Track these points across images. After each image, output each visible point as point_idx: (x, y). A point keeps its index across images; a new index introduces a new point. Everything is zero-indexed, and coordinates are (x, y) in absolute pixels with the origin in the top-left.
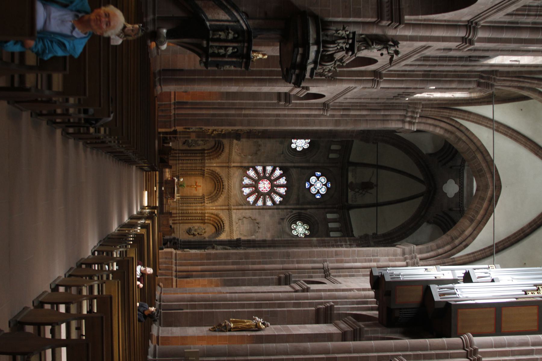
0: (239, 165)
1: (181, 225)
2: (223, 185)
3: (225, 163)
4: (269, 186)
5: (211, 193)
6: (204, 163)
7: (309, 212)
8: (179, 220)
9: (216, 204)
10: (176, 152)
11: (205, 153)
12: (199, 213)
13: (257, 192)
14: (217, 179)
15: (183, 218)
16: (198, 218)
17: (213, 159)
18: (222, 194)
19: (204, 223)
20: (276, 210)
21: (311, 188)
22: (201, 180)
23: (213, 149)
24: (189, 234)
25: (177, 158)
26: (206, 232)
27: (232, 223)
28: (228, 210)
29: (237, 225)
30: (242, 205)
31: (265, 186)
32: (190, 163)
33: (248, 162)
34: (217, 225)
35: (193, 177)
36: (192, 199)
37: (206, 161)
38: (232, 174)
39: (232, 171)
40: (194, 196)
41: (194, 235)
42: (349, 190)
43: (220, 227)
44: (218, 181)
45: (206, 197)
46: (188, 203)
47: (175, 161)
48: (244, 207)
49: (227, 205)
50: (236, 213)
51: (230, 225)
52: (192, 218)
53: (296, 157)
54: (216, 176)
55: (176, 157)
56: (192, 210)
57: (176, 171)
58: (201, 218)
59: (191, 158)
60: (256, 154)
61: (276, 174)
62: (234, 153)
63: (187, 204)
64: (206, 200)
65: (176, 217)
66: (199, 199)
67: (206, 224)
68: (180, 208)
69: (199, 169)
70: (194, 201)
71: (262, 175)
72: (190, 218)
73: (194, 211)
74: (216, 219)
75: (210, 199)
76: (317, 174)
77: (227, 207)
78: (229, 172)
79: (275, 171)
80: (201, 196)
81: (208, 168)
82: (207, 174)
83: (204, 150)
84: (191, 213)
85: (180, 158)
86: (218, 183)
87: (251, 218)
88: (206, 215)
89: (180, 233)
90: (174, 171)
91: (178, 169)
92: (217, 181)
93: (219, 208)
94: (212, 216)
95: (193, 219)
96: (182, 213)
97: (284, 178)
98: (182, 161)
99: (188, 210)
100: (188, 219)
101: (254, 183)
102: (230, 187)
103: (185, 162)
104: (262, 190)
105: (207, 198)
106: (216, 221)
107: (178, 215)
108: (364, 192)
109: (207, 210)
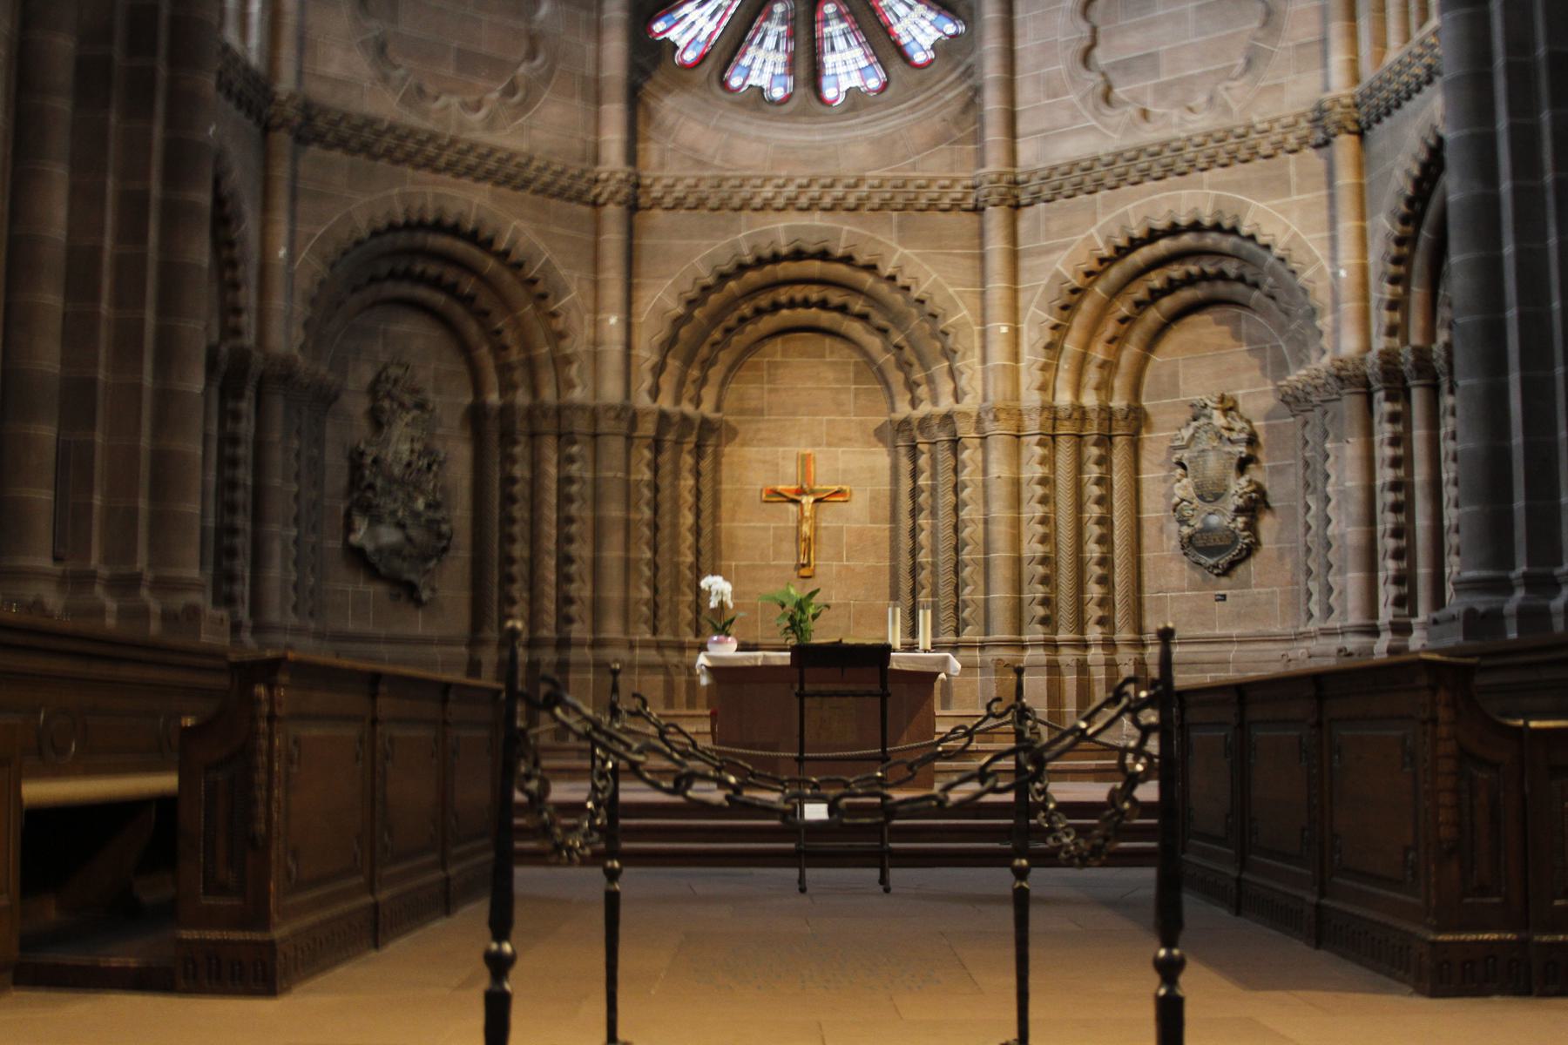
0: (614, 113)
2: (798, 255)
3: (597, 232)
5: (872, 371)
6: (594, 414)
8: (1109, 644)
9: (962, 315)
11: (507, 411)
12: (1042, 462)
15: (1093, 612)
16: (1093, 472)
18: (871, 268)
19: (1137, 419)
22: (751, 452)
23: (472, 329)
24: (1251, 550)
27: (1141, 150)
28: (1017, 207)
29: (1155, 110)
30: (977, 91)
32: (598, 544)
33: (597, 31)
34: (1155, 295)
35: (725, 525)
36: (914, 533)
37: (578, 395)
38: (690, 175)
40: (894, 517)
41: (1255, 505)
43: (1176, 271)
45: (903, 409)
46: (957, 568)
48: (991, 70)
49: (969, 220)
50: (1049, 135)
51: (1168, 170)
52: (1093, 531)
54: (715, 319)
56: (1016, 524)
57: (665, 668)
58: (1093, 452)
59: (550, 530)
62: (507, 139)
64: (925, 409)
65: (1083, 668)
66: (915, 474)
67: (1145, 403)
68: (1001, 632)
69: (655, 468)
70: (933, 513)
72: (1093, 551)
73: (1033, 511)
74: (1104, 309)
75: (918, 375)
77: (995, 218)
78: (678, 204)
81: (648, 381)
82: (697, 402)
83: (476, 416)
84: (1044, 540)
85: (548, 632)
86: (776, 307)
88: (1064, 398)
89: (1235, 631)
90: (670, 689)
91: (652, 656)
92: (759, 312)
93: (997, 286)
95: (1105, 521)
96: (1045, 621)
98: (574, 610)
99: (1018, 561)
100: (1105, 561)
102: (815, 191)
103: (581, 590)
105: (914, 403)
106: (1124, 309)
107: (1067, 657)
109: (1016, 397)
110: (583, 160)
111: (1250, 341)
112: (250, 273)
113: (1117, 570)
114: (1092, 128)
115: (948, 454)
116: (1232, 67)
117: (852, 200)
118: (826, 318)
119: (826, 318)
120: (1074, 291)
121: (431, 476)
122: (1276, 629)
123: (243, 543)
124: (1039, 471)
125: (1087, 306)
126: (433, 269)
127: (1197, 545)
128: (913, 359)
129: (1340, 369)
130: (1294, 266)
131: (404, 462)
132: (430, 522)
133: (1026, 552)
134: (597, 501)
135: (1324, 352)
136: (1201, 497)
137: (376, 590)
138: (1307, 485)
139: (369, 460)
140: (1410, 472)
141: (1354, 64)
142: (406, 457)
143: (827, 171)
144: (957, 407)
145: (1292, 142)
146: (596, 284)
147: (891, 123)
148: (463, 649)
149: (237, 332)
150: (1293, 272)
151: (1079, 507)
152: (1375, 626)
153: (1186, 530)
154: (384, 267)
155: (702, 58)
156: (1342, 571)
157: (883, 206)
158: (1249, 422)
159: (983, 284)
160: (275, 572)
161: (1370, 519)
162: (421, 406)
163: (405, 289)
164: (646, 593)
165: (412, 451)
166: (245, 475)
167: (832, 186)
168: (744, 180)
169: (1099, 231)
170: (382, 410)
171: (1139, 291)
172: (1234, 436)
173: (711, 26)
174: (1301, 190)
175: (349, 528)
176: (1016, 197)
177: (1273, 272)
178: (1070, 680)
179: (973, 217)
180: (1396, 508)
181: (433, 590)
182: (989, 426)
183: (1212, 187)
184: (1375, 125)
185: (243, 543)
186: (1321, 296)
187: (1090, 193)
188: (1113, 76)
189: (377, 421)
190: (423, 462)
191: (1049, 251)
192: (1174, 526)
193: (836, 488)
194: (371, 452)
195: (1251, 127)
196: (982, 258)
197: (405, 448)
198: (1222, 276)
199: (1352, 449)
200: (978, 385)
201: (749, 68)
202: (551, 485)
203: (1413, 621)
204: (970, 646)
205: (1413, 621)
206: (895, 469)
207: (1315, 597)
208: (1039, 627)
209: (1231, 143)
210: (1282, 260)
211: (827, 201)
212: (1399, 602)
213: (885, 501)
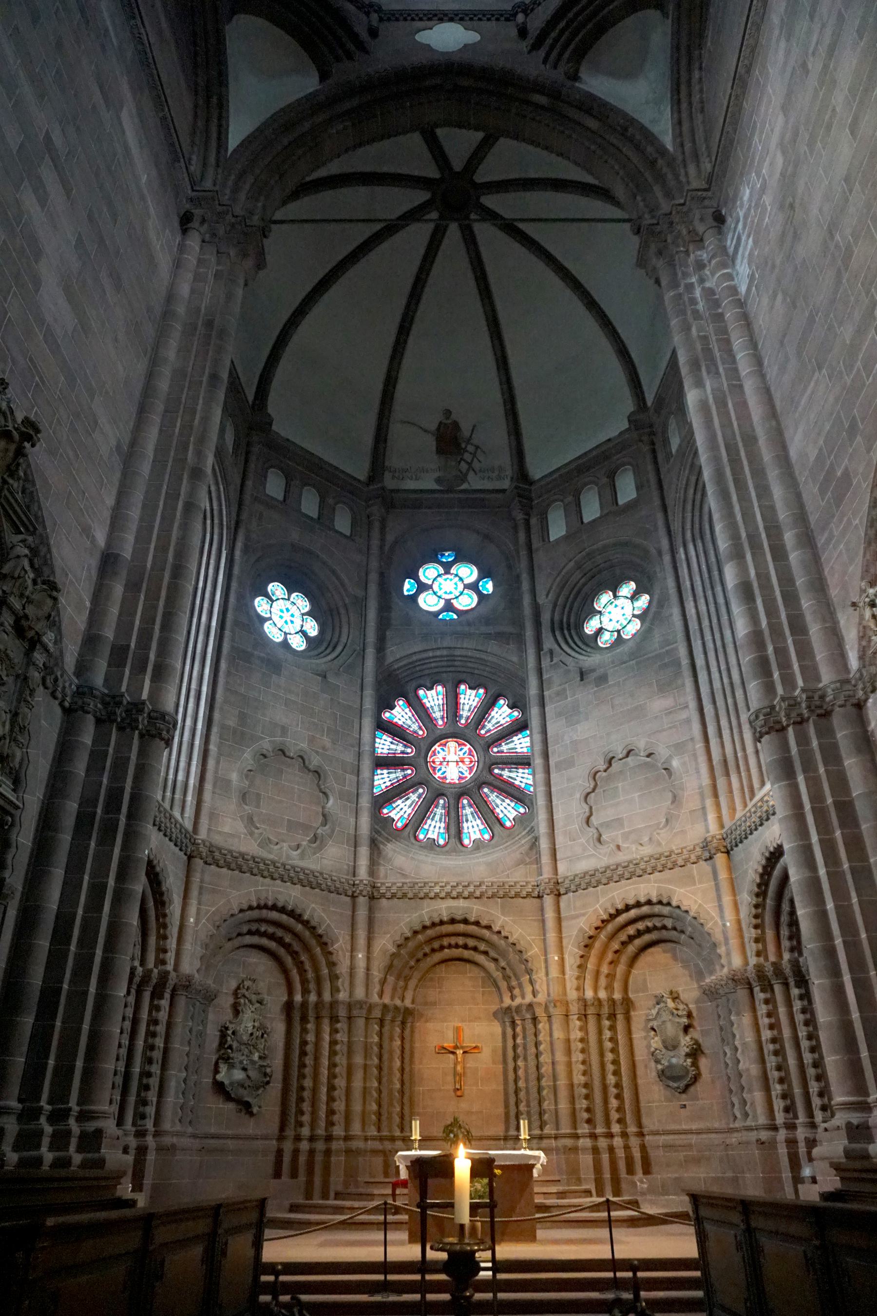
0: (364, 851)
1: (649, 1124)
2: (453, 921)
4: (452, 744)
6: (350, 1006)
7: (547, 595)
8: (624, 1135)
9: (534, 951)
10: (287, 1159)
11: (304, 1005)
12: (581, 1029)
13: (480, 787)
14: (427, 949)
15: (615, 1116)
16: (607, 1034)
17: (332, 965)
18: (488, 927)
19: (628, 1004)
20: (547, 709)
21: (460, 607)
22: (430, 1025)
23: (289, 961)
24: (696, 1078)
25: (320, 1146)
26: (671, 993)
27: (618, 865)
28: (559, 895)
29: (624, 845)
30: (536, 839)
31: (452, 757)
34: (631, 938)
35: (417, 1067)
36: (515, 1070)
38: (400, 881)
39: (388, 879)
40: (505, 1061)
41: (695, 1052)
42: (464, 486)
43: (641, 926)
44: (436, 945)
45: (507, 1001)
46: (540, 1089)
47: (333, 1159)
48: (543, 829)
52: (610, 1068)
53: (344, 639)
54: (412, 955)
55: (312, 1152)
56: (569, 1064)
58: (606, 1023)
59: (324, 1072)
60: (317, 773)
61: (409, 722)
62: (311, 864)
63: (545, 1093)
64: (518, 1001)
65: (611, 1149)
66: (514, 1037)
67: (631, 995)
68: (565, 1130)
69: (380, 1035)
70: (525, 1059)
71: (409, 772)
72: (611, 1079)
73: (578, 1057)
74: (606, 946)
75: (514, 983)
76: (408, 590)
77: (548, 900)
78: (394, 896)
79: (396, 724)
80: (503, 1023)
83: (289, 1007)
84: (584, 1073)
85: (321, 1132)
86: (442, 948)
87: (588, 794)
88: (589, 994)
89: (694, 1126)
91: (377, 1145)
92: (433, 950)
93: (551, 936)
94: (591, 966)
96: (589, 1121)
97: (421, 693)
99: (571, 1086)
100: (618, 1085)
101: (441, 802)
103: (340, 1106)
104: (471, 769)
106: (616, 946)
108: (470, 448)
109: (565, 993)
110: (347, 875)
111: (682, 961)
112: (173, 931)
113: (625, 1090)
114: (593, 855)
115: (531, 1026)
116: (660, 823)
117: (478, 894)
118: (466, 954)
119: (466, 954)
120: (590, 937)
121: (263, 1040)
122: (716, 1125)
123: (154, 1082)
124: (579, 1034)
125: (598, 945)
126: (271, 930)
127: (667, 1075)
128: (512, 975)
129: (734, 975)
130: (702, 921)
131: (250, 1032)
132: (262, 1066)
133: (576, 1081)
134: (350, 1053)
135: (723, 966)
136: (666, 1048)
137: (231, 1106)
138: (723, 1040)
139: (229, 1032)
140: (780, 1031)
141: (720, 818)
142: (250, 1030)
143: (465, 879)
144: (535, 1000)
145: (693, 858)
146: (353, 937)
147: (495, 855)
148: (274, 1142)
149: (163, 962)
150: (702, 924)
151: (602, 1055)
152: (775, 1125)
153: (660, 1067)
154: (245, 929)
155: (406, 825)
156: (750, 1091)
157: (493, 896)
158: (687, 1005)
159: (544, 935)
160: (171, 1098)
161: (762, 1061)
162: (260, 1002)
163: (255, 940)
164: (374, 1107)
165: (254, 1027)
166: (159, 1042)
167: (468, 885)
168: (425, 883)
169: (600, 906)
170: (240, 1004)
171: (623, 937)
172: (680, 1013)
173: (409, 811)
174: (700, 883)
175: (216, 1071)
176: (558, 890)
177: (691, 925)
178: (605, 1157)
179: (538, 900)
180: (776, 1053)
181: (260, 1107)
182: (552, 1010)
183: (655, 882)
184: (735, 849)
185: (154, 1082)
186: (718, 936)
187: (594, 887)
188: (600, 829)
189: (236, 1010)
190: (259, 1033)
191: (577, 917)
192: (653, 1064)
193: (474, 1045)
194: (232, 1027)
195: (671, 852)
196: (543, 921)
197: (250, 1025)
198: (664, 927)
199: (746, 1019)
200: (545, 988)
201: (428, 830)
202: (326, 1045)
203: (797, 1121)
204: (549, 1137)
205: (797, 1121)
206: (504, 1034)
207: (737, 1106)
208: (586, 1125)
209: (663, 860)
210: (695, 918)
211: (466, 894)
212: (787, 1110)
213: (500, 1052)
